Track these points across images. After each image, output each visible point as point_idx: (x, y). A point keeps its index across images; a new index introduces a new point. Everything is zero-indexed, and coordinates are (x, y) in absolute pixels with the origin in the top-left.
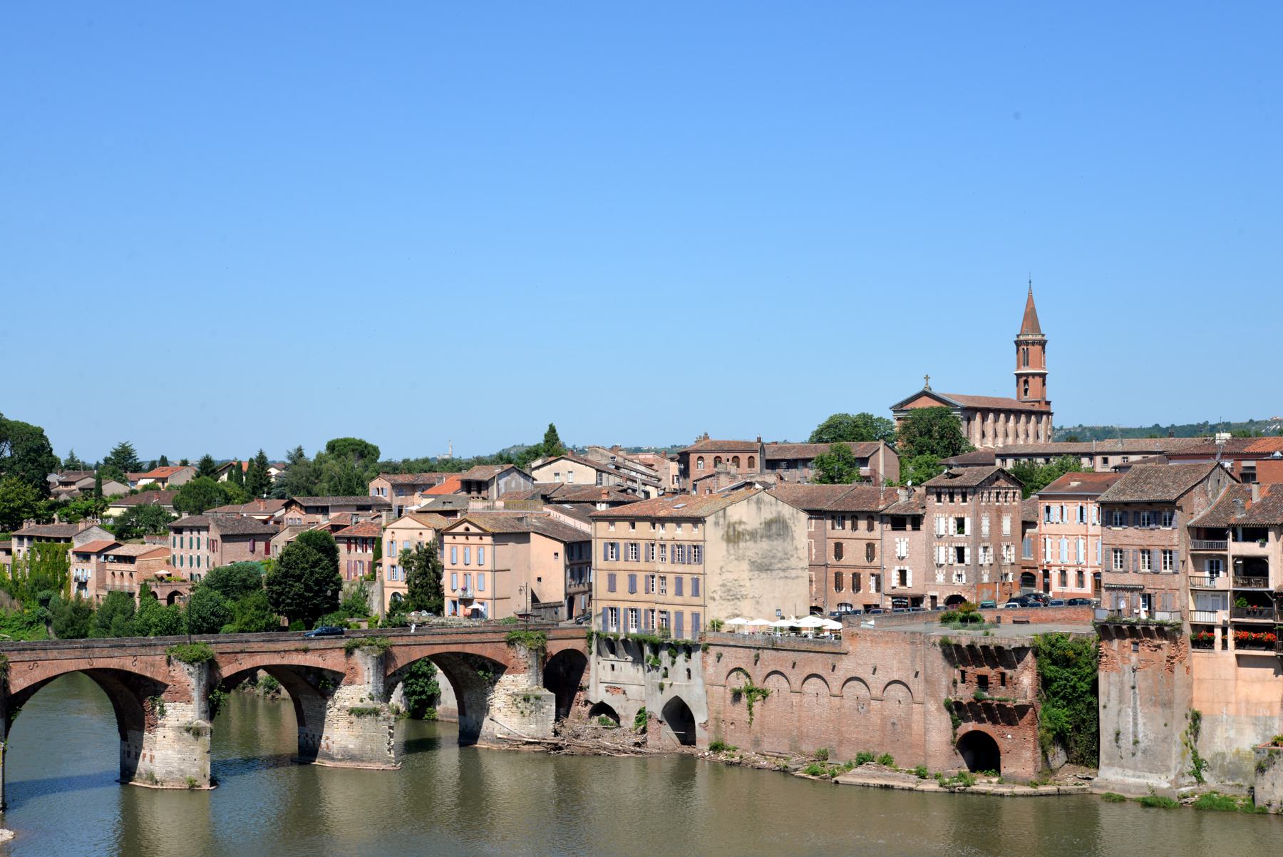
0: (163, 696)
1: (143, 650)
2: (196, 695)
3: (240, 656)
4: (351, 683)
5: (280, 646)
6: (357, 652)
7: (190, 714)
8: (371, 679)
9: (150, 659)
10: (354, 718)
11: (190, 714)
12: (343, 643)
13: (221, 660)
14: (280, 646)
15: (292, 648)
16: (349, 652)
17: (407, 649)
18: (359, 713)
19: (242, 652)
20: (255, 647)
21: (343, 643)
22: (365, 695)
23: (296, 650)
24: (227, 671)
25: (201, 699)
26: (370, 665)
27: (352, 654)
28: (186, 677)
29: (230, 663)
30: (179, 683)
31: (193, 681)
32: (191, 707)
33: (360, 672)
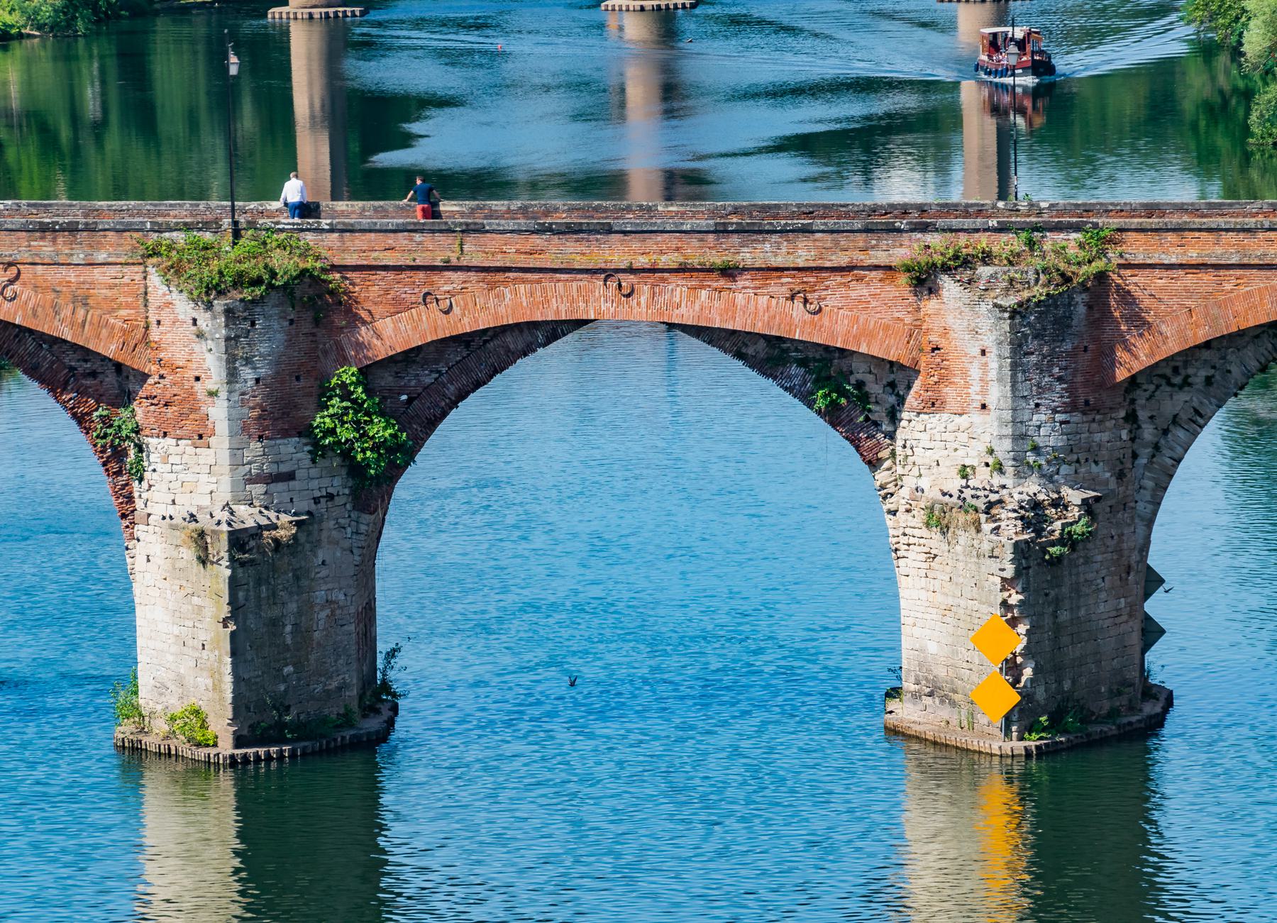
0: (141, 411)
1: (45, 248)
2: (218, 413)
3: (447, 283)
4: (933, 405)
5: (615, 252)
6: (949, 286)
7: (205, 483)
8: (998, 394)
9: (71, 275)
10: (935, 540)
11: (205, 483)
12: (904, 250)
13: (368, 292)
14: (615, 252)
15: (670, 260)
16: (924, 280)
17: (1207, 277)
18: (938, 519)
19: (448, 267)
20: (510, 250)
21: (904, 250)
22: (974, 456)
23: (683, 270)
24: (391, 331)
25: (241, 430)
26: (989, 340)
27: (933, 291)
28: (187, 340)
29: (399, 306)
30: (175, 369)
31: (210, 362)
32: (206, 456)
33: (954, 365)
